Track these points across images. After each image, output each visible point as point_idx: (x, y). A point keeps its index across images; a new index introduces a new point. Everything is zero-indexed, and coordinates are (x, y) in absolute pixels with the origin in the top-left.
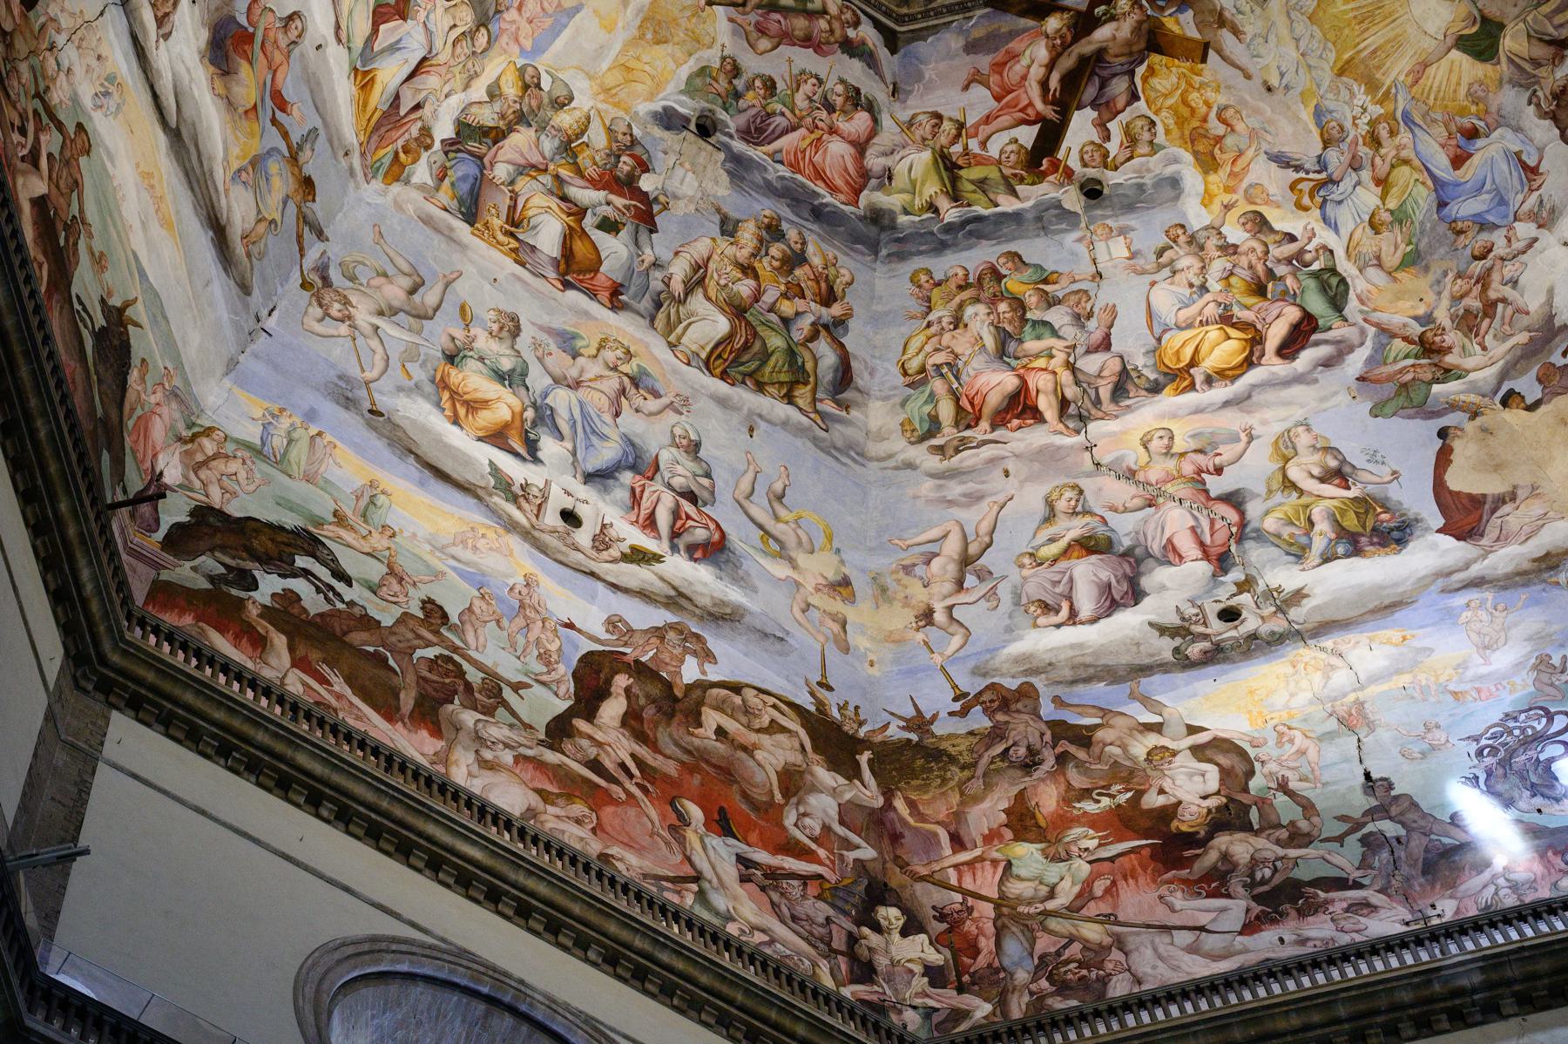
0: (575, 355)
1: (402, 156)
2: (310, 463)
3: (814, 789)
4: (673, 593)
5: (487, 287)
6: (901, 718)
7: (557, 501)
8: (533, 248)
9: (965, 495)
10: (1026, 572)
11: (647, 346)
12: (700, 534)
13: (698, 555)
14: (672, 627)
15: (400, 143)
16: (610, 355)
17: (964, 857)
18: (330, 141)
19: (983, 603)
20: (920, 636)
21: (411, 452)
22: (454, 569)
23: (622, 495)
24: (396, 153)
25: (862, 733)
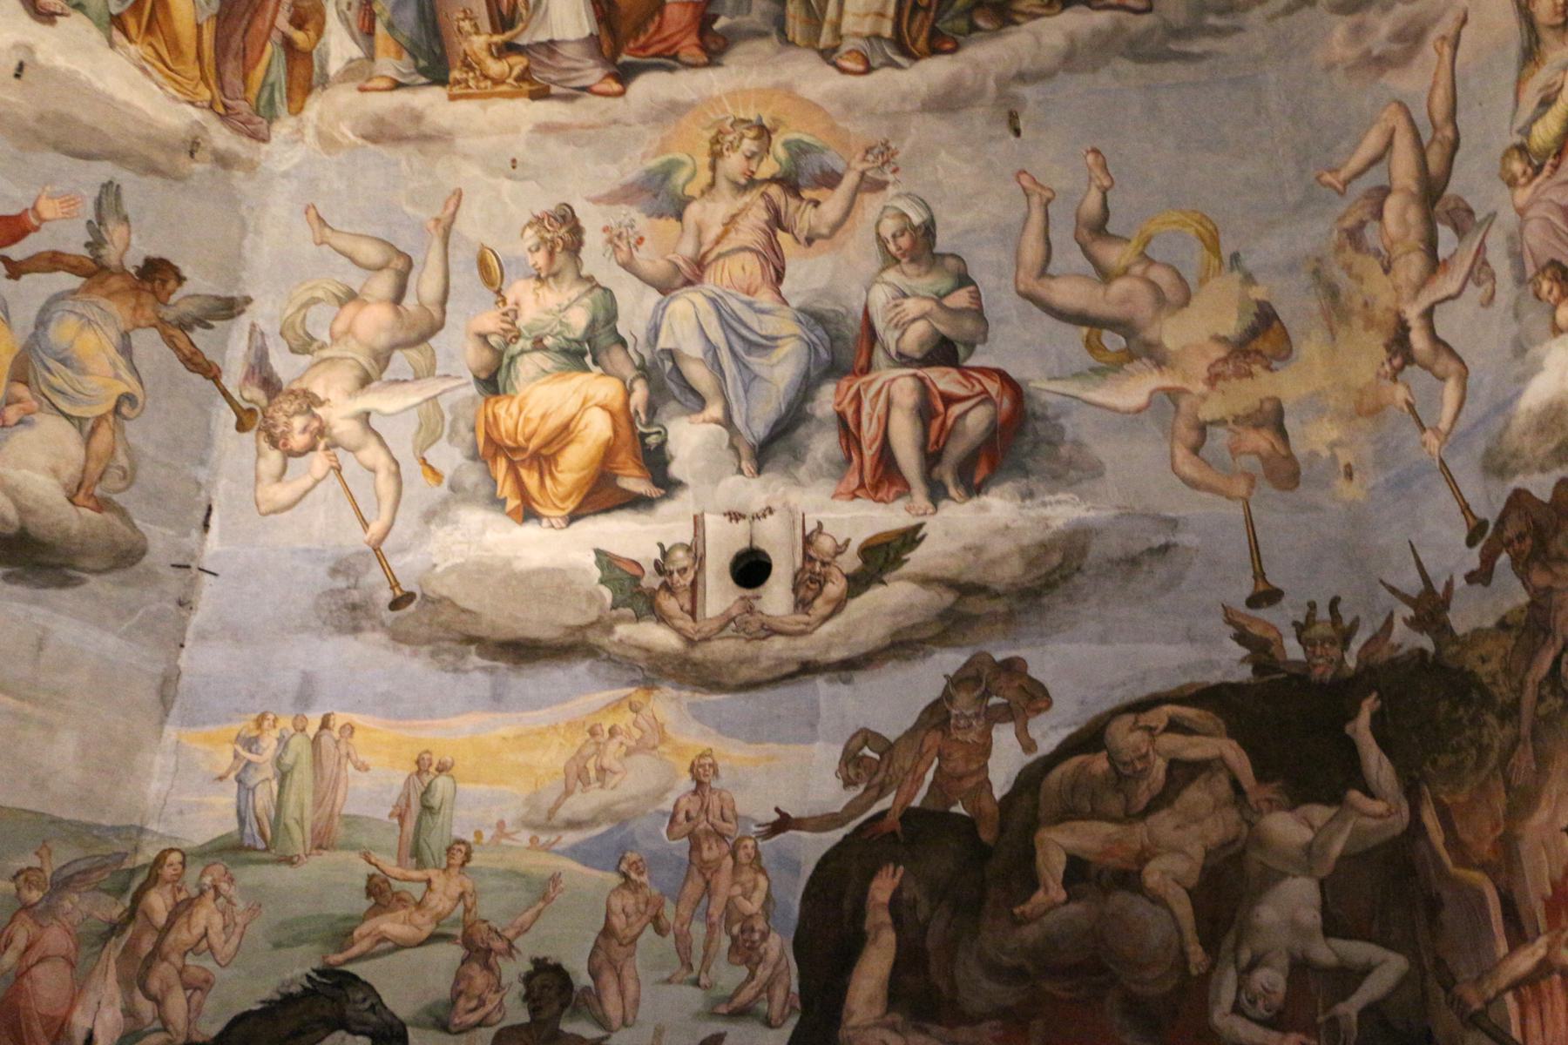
0: (677, 209)
1: (299, 37)
2: (318, 804)
3: (1270, 879)
4: (949, 598)
5: (507, 185)
6: (1405, 599)
7: (723, 542)
8: (551, 46)
9: (1398, 36)
10: (1523, 195)
11: (788, 90)
12: (977, 420)
13: (981, 473)
14: (957, 682)
15: (282, 22)
16: (733, 163)
17: (1524, 962)
18: (152, 169)
19: (1474, 293)
20: (1400, 393)
21: (470, 640)
22: (574, 852)
23: (823, 444)
24: (288, 44)
25: (1351, 662)
